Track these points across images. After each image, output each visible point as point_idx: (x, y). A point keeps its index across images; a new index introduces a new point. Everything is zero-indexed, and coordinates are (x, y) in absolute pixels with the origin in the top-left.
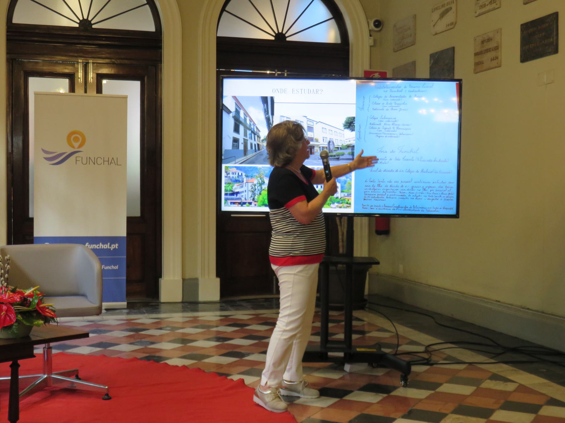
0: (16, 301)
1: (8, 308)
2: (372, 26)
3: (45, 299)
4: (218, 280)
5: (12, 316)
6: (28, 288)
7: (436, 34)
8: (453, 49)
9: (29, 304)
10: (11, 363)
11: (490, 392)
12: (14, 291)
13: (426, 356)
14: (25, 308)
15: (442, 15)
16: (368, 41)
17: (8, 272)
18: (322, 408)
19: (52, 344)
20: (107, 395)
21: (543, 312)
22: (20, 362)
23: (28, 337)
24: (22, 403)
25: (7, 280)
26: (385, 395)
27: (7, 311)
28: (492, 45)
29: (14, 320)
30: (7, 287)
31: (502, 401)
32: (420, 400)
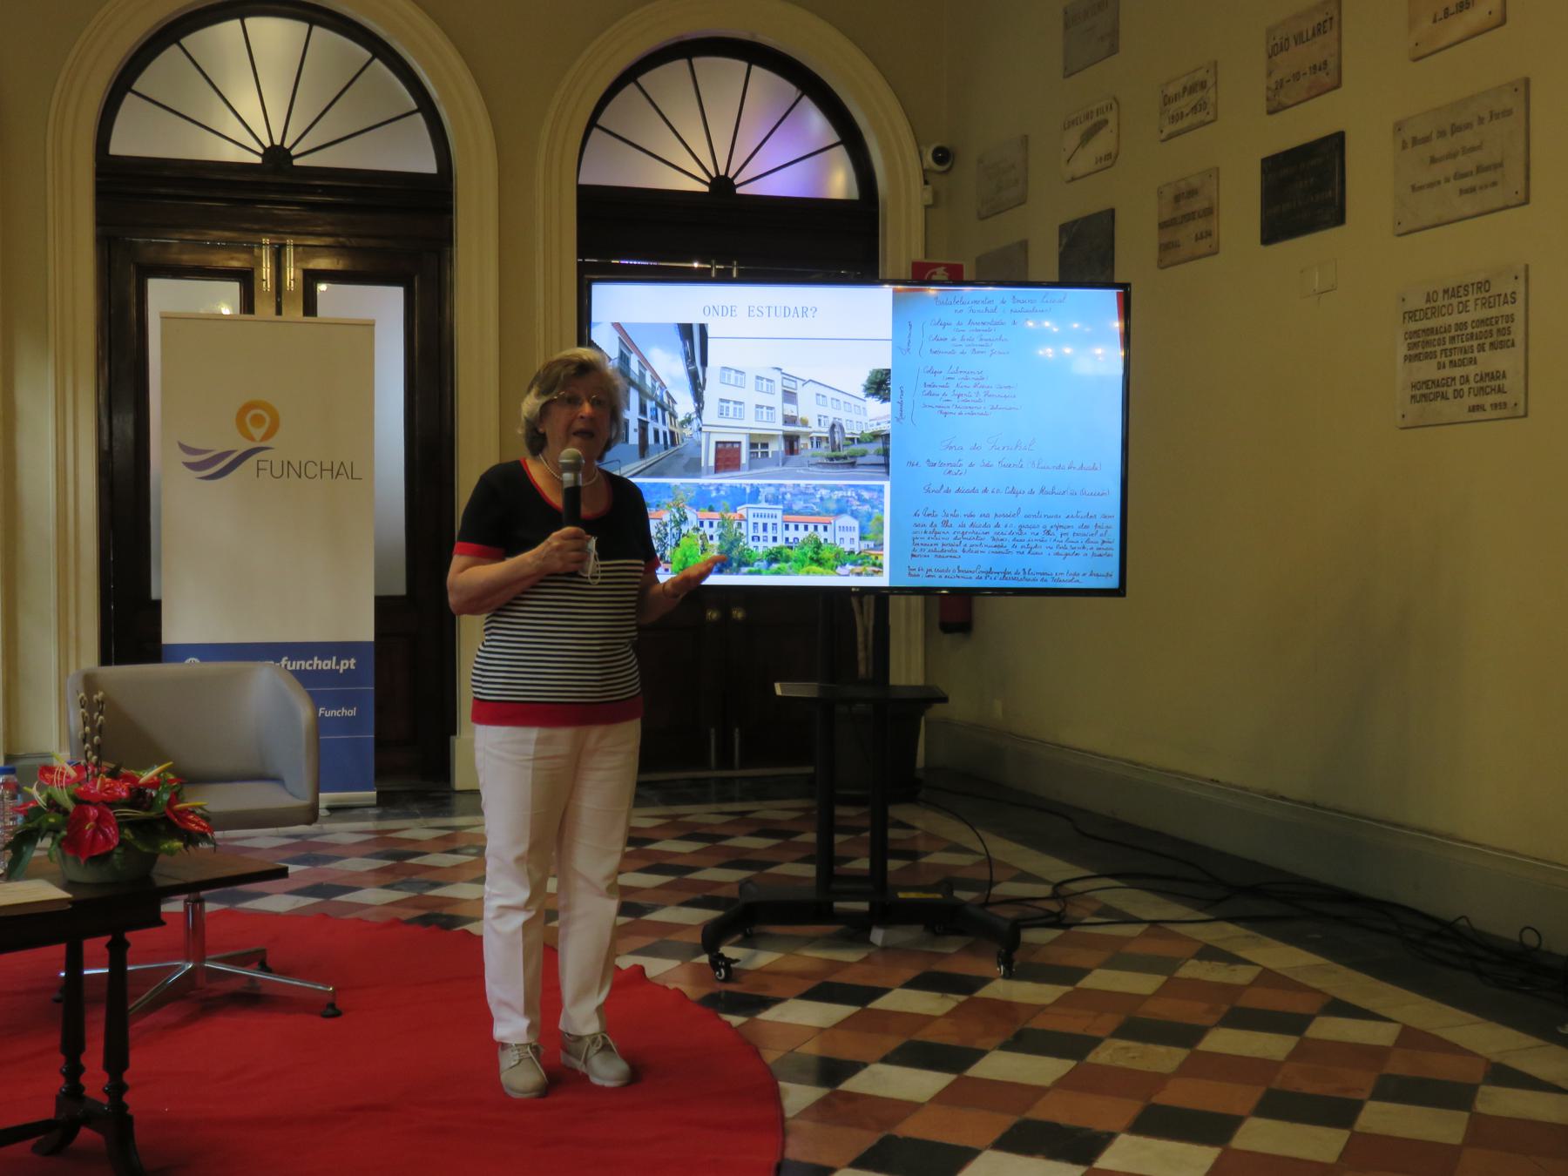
0: (120, 797)
1: (101, 812)
2: (929, 158)
3: (187, 790)
5: (111, 831)
7: (1073, 179)
8: (1113, 211)
9: (150, 803)
10: (108, 938)
11: (1197, 988)
12: (114, 774)
13: (1054, 907)
14: (141, 814)
15: (1088, 136)
17: (100, 731)
18: (821, 1030)
19: (202, 893)
20: (332, 1006)
21: (1315, 806)
22: (129, 936)
24: (135, 1029)
25: (97, 749)
26: (962, 998)
27: (98, 820)
28: (1198, 204)
29: (116, 842)
30: (97, 765)
31: (1225, 1008)
32: (1040, 1009)
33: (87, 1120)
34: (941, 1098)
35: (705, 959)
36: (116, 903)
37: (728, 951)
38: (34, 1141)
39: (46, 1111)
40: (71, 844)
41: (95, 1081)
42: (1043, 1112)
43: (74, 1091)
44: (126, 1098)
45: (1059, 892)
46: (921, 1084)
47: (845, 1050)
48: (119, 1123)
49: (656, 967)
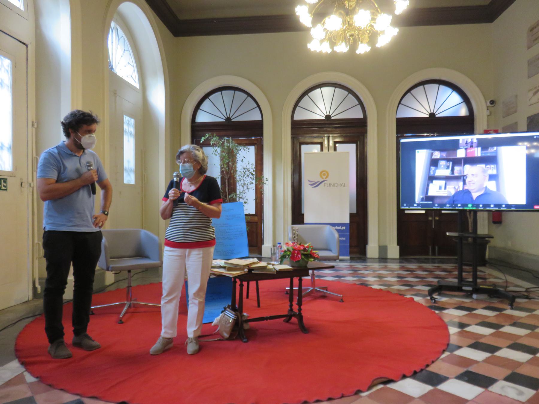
4: (398, 247)
5: (299, 256)
6: (306, 243)
7: (531, 105)
9: (307, 251)
10: (298, 278)
12: (300, 244)
13: (526, 294)
14: (305, 253)
16: (486, 113)
18: (459, 316)
19: (316, 272)
20: (342, 300)
22: (303, 278)
23: (306, 266)
24: (303, 299)
32: (521, 318)
33: (294, 315)
34: (492, 335)
35: (429, 298)
36: (300, 271)
37: (435, 296)
38: (283, 319)
39: (286, 313)
40: (293, 258)
41: (295, 308)
42: (520, 341)
43: (291, 310)
44: (302, 312)
45: (527, 290)
46: (487, 331)
47: (466, 321)
48: (300, 317)
49: (416, 299)
